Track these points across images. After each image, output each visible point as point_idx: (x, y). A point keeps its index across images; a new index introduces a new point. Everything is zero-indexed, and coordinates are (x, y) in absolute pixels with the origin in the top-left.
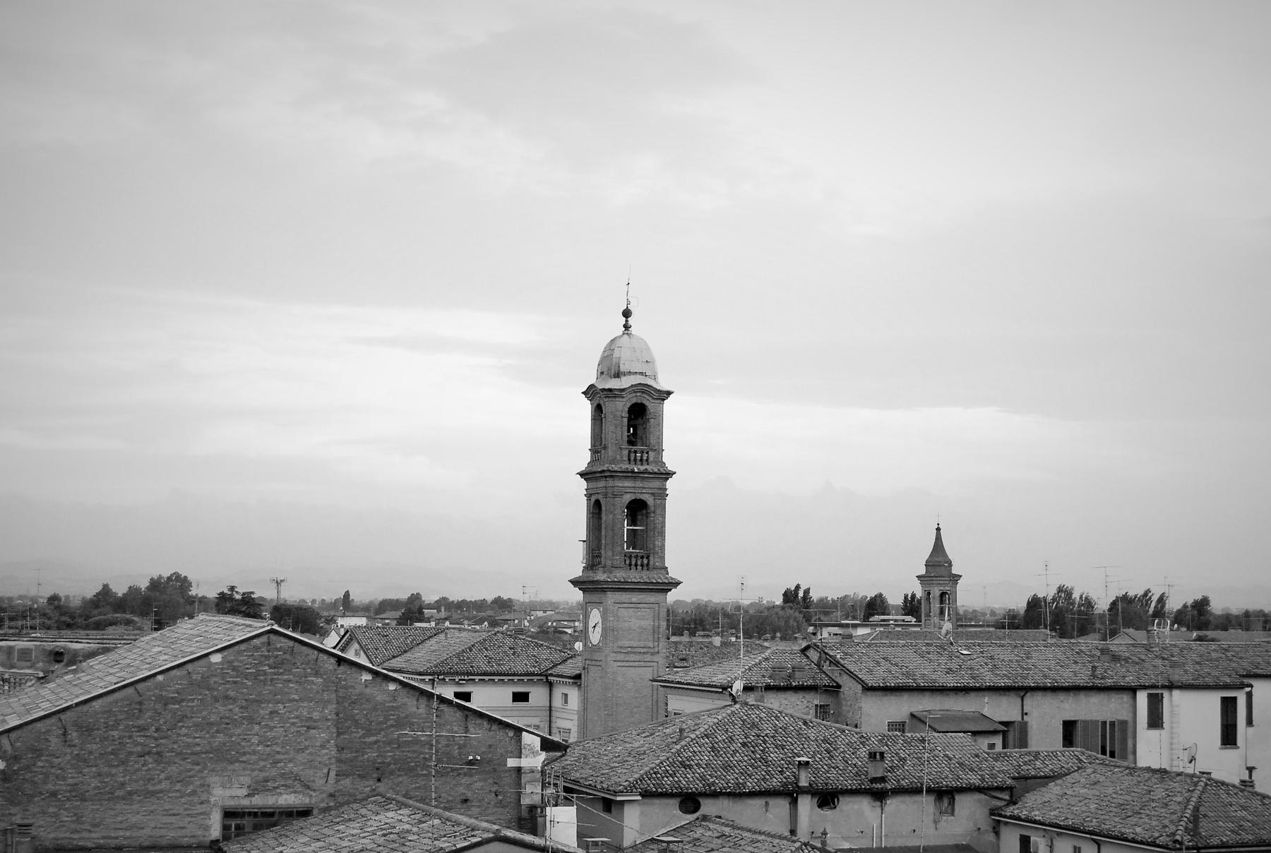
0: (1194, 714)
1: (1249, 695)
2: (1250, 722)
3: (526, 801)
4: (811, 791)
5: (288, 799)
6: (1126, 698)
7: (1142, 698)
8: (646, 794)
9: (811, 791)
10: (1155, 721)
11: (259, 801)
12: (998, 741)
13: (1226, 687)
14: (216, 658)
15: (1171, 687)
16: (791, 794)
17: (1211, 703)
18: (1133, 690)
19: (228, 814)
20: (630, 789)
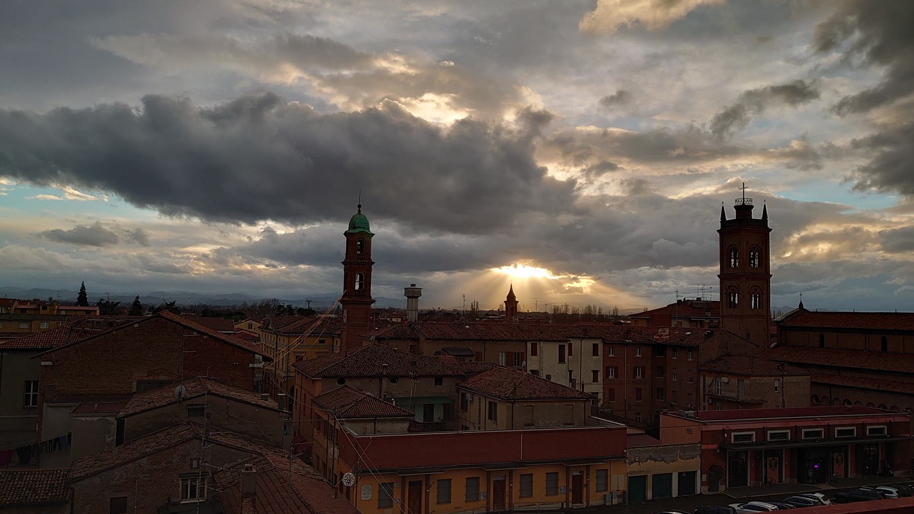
0: (549, 351)
1: (570, 345)
2: (570, 354)
3: (255, 380)
4: (387, 376)
5: (163, 378)
6: (523, 344)
7: (529, 345)
8: (324, 377)
9: (387, 376)
10: (534, 353)
11: (150, 378)
12: (473, 359)
13: (561, 341)
14: (136, 326)
15: (540, 341)
16: (380, 377)
17: (555, 347)
18: (526, 341)
19: (138, 382)
20: (316, 376)
